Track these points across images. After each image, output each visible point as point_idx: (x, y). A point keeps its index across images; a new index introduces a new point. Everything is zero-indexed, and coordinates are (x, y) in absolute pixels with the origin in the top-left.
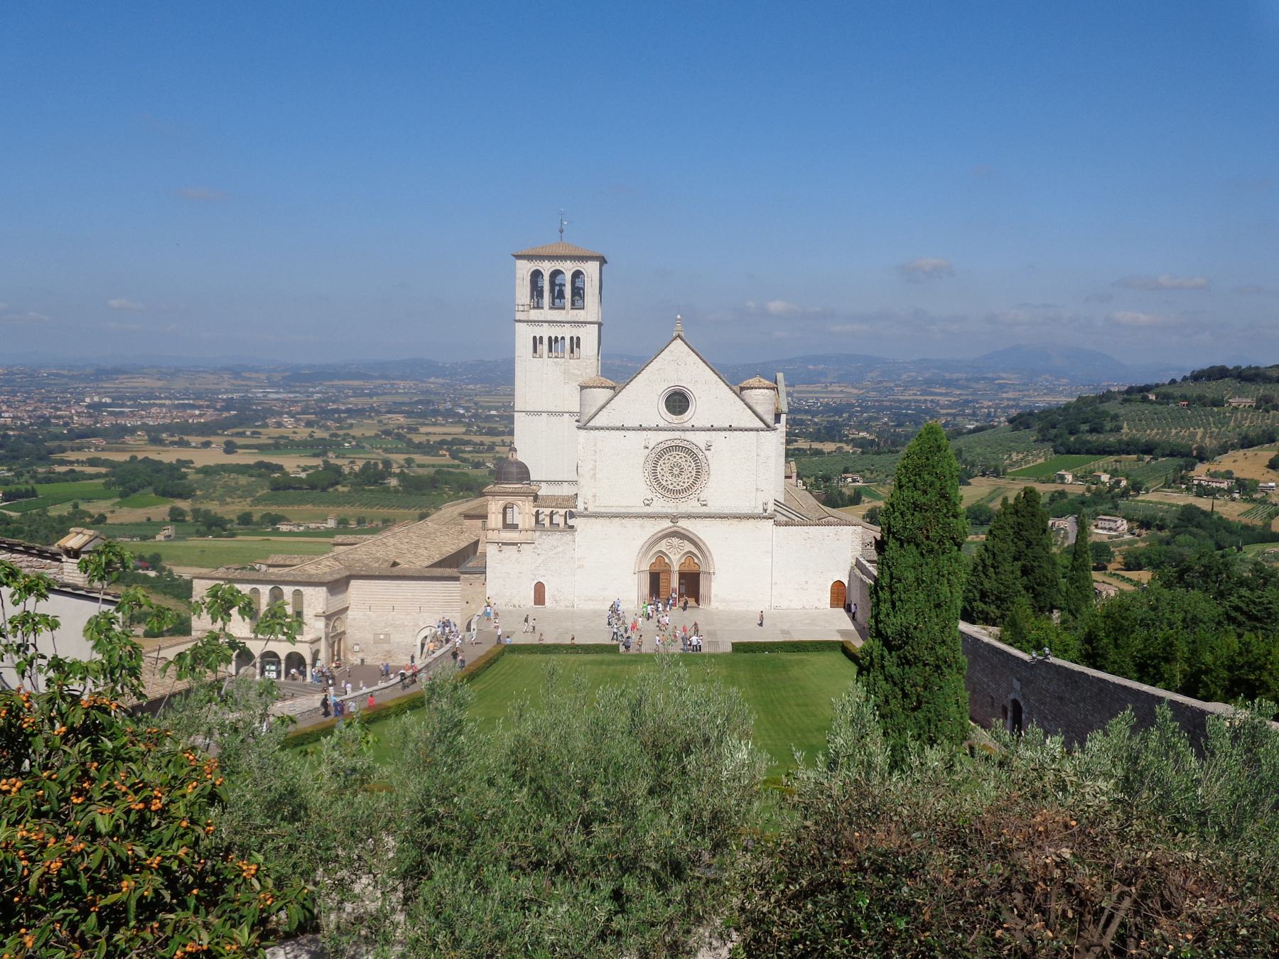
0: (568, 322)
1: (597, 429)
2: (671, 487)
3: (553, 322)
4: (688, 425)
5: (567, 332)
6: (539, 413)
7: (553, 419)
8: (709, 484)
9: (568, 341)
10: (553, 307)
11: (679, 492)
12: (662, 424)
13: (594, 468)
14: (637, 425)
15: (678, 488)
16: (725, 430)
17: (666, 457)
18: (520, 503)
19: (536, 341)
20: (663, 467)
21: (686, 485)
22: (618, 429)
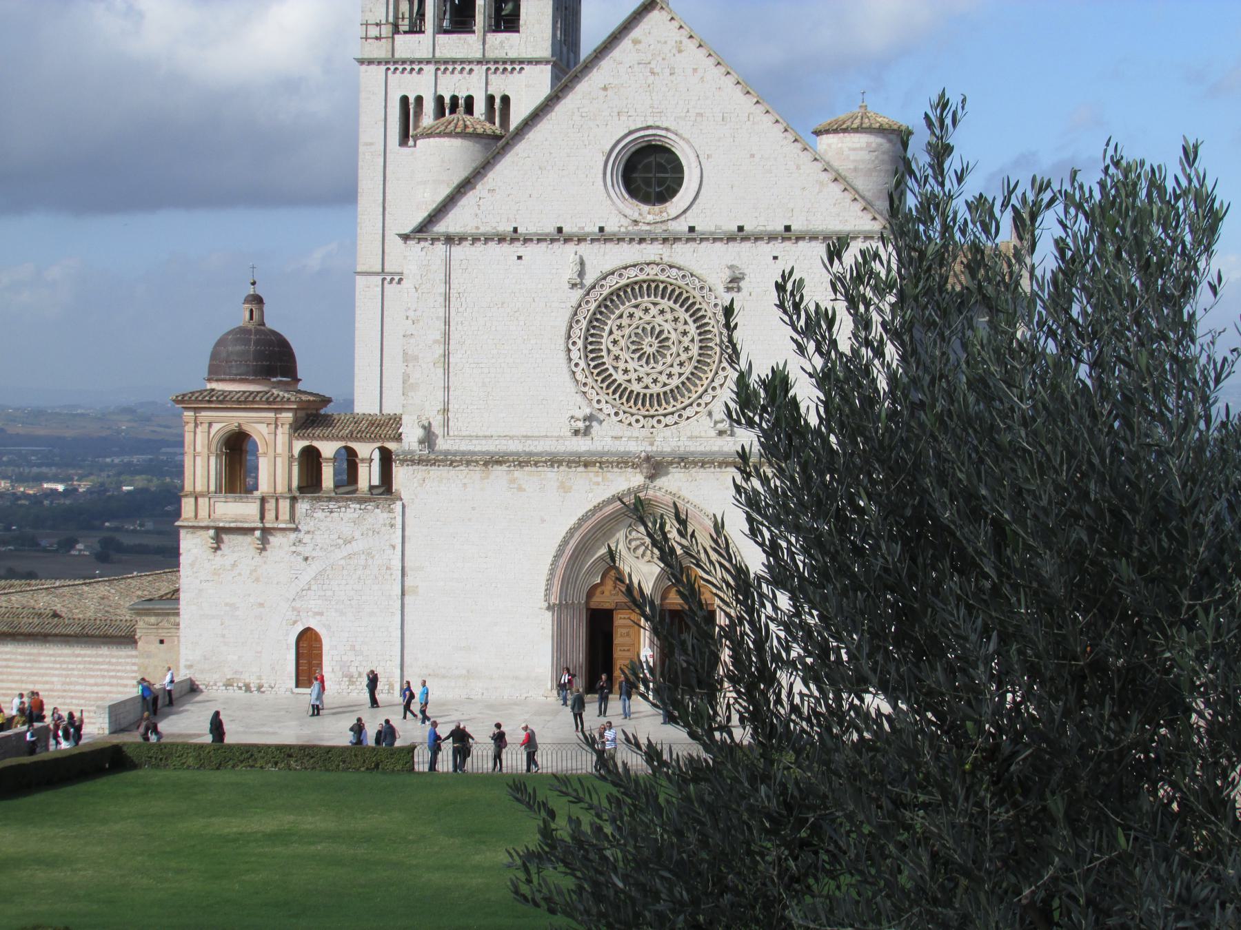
0: (479, 62)
1: (449, 239)
2: (636, 387)
4: (681, 226)
11: (658, 399)
14: (550, 229)
15: (656, 389)
16: (772, 238)
17: (626, 308)
18: (263, 428)
19: (408, 109)
21: (675, 382)
22: (501, 240)
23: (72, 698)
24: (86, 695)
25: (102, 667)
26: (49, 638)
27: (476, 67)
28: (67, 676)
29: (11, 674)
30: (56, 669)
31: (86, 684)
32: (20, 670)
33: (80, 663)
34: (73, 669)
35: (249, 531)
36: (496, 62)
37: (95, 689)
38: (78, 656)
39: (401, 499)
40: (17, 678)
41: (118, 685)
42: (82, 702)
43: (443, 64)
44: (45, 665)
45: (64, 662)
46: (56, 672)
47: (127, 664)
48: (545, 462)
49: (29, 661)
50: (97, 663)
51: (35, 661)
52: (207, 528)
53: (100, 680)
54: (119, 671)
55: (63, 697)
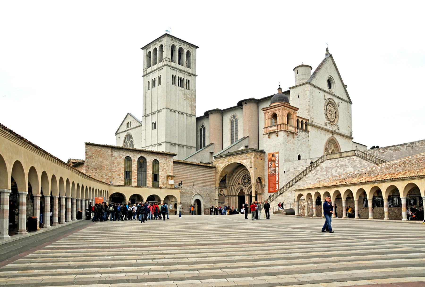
0: (186, 72)
2: (330, 119)
3: (181, 70)
4: (334, 94)
5: (186, 77)
6: (175, 111)
7: (181, 116)
8: (339, 121)
9: (185, 81)
10: (179, 64)
12: (328, 91)
13: (312, 104)
15: (332, 120)
17: (328, 106)
19: (174, 77)
20: (328, 110)
23: (192, 180)
26: (187, 165)
27: (185, 73)
28: (190, 174)
29: (179, 173)
30: (188, 172)
31: (194, 177)
32: (181, 172)
33: (193, 171)
34: (191, 173)
35: (293, 133)
36: (188, 73)
37: (196, 178)
38: (193, 170)
39: (309, 132)
40: (181, 174)
41: (200, 177)
43: (180, 70)
44: (186, 171)
46: (188, 173)
47: (202, 172)
49: (183, 170)
50: (196, 172)
51: (184, 170)
52: (287, 132)
53: (197, 176)
54: (200, 174)
55: (190, 179)
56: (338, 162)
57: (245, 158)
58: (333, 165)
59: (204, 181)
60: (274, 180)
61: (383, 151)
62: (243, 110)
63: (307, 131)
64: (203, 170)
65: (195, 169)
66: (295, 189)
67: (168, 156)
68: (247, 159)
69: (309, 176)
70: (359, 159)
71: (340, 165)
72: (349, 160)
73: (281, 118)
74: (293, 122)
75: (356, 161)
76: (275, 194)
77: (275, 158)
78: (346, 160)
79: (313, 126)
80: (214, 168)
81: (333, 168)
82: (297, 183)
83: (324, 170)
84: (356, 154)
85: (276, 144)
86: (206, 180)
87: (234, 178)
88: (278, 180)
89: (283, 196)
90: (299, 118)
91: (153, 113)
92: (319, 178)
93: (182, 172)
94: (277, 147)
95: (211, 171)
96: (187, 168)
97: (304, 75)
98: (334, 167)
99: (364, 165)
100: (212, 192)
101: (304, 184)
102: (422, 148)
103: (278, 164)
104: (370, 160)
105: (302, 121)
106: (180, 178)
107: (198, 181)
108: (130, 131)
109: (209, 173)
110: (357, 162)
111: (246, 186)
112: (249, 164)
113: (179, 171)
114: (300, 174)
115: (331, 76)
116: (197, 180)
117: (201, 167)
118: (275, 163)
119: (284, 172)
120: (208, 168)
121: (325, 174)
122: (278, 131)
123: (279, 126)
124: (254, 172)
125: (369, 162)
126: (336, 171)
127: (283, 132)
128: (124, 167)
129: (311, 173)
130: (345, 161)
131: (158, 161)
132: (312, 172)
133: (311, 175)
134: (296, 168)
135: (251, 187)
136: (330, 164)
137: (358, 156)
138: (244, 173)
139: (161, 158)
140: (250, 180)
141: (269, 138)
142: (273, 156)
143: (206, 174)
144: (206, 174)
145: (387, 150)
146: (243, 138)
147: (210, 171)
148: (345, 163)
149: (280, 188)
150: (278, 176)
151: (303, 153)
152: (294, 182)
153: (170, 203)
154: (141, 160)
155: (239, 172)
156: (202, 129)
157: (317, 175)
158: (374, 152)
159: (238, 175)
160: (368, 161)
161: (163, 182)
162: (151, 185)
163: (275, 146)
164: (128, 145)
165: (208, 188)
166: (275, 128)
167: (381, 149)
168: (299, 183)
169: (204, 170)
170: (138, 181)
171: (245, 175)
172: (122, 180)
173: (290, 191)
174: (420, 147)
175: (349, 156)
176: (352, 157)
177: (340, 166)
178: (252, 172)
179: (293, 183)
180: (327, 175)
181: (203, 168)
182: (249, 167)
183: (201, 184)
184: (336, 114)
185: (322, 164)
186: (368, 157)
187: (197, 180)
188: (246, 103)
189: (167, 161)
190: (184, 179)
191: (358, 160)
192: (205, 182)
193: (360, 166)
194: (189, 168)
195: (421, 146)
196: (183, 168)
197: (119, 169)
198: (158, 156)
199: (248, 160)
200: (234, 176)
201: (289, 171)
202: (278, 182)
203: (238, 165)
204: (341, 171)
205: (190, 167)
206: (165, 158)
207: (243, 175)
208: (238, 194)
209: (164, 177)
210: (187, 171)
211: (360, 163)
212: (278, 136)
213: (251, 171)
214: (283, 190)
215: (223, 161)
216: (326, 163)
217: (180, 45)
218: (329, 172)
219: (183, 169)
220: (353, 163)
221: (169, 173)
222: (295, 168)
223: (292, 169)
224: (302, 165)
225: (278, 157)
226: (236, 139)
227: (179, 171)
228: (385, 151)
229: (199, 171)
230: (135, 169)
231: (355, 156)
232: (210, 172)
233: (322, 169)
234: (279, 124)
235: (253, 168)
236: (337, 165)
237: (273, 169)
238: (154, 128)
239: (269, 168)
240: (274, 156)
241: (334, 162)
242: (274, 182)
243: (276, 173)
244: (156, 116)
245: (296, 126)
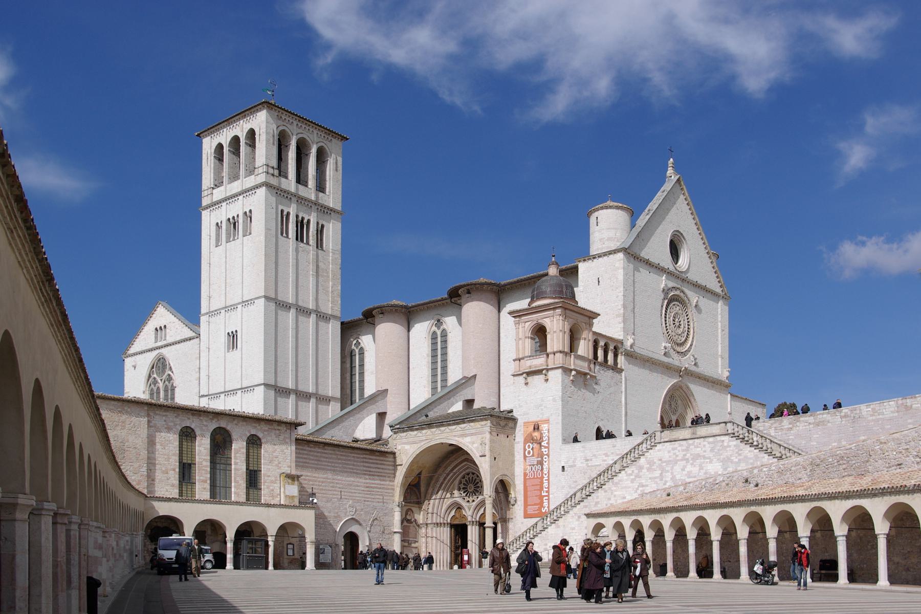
15: (679, 342)
21: (683, 339)
23: (337, 483)
24: (343, 482)
25: (350, 467)
26: (326, 447)
33: (340, 463)
34: (337, 467)
38: (339, 459)
42: (341, 486)
45: (333, 463)
46: (329, 468)
48: (659, 364)
49: (316, 460)
50: (347, 464)
54: (357, 470)
56: (687, 450)
57: (467, 432)
58: (677, 456)
59: (367, 487)
60: (538, 487)
61: (791, 426)
62: (461, 309)
63: (615, 368)
64: (364, 460)
65: (344, 458)
66: (587, 511)
67: (284, 425)
68: (472, 434)
69: (620, 481)
70: (735, 442)
71: (691, 455)
72: (712, 445)
73: (555, 337)
74: (584, 348)
75: (730, 446)
76: (540, 522)
77: (541, 434)
78: (706, 444)
79: (631, 356)
80: (392, 456)
81: (676, 462)
82: (592, 495)
83: (654, 467)
84: (729, 432)
85: (542, 401)
86: (373, 484)
87: (441, 479)
88: (548, 488)
89: (558, 527)
90: (599, 338)
91: (232, 308)
92: (643, 486)
93: (313, 464)
94: (545, 407)
95: (385, 463)
96: (327, 456)
97: (613, 229)
98: (678, 460)
99: (746, 457)
100: (386, 514)
101: (609, 499)
102: (873, 420)
103: (547, 450)
104: (760, 446)
105: (606, 345)
106: (310, 480)
107: (353, 488)
108: (164, 351)
109: (379, 468)
110: (731, 449)
111: (471, 499)
112: (477, 448)
113: (306, 463)
114: (600, 475)
115: (678, 231)
116: (351, 485)
117: (359, 452)
118: (541, 446)
119: (563, 467)
120: (378, 456)
121: (659, 475)
122: (548, 370)
123: (551, 356)
124: (491, 467)
125: (757, 450)
126: (683, 470)
127: (560, 371)
128: (178, 452)
129: (626, 472)
130: (704, 446)
131: (260, 439)
132: (628, 470)
133: (625, 478)
134: (591, 460)
135: (482, 503)
136: (669, 452)
137: (732, 437)
138: (465, 470)
139: (267, 431)
140: (479, 487)
141: (526, 384)
142: (537, 428)
143: (371, 470)
144: (371, 470)
145: (798, 424)
146: (461, 379)
147: (383, 462)
148: (705, 451)
149: (552, 507)
150: (548, 477)
151: (609, 421)
152: (587, 491)
153: (289, 542)
154: (217, 437)
155: (452, 466)
156: (357, 351)
157: (640, 477)
158: (770, 428)
159: (448, 475)
160: (755, 449)
161: (273, 490)
162: (243, 498)
163: (541, 405)
164: (158, 388)
165: (377, 504)
166: (539, 362)
167: (785, 422)
168: (598, 497)
169: (367, 460)
170: (211, 486)
171: (468, 474)
172: (173, 485)
173: (575, 514)
174: (871, 418)
175: (714, 436)
176: (719, 438)
177: (692, 459)
178: (485, 468)
179: (584, 496)
180: (661, 480)
181: (364, 456)
182: (478, 455)
183: (361, 495)
184: (688, 325)
185: (650, 451)
186: (755, 439)
187: (351, 485)
188: (469, 292)
189: (282, 438)
190: (319, 482)
191: (732, 446)
192: (370, 489)
193: (737, 460)
194: (331, 454)
195: (872, 415)
196: (315, 454)
197: (166, 457)
198: (259, 427)
199: (474, 437)
200: (441, 475)
201: (575, 466)
202: (547, 492)
203: (451, 448)
204: (695, 470)
205: (333, 452)
206: (278, 432)
207: (462, 474)
208: (449, 521)
209: (273, 479)
210: (326, 462)
211: (737, 453)
212: (547, 380)
213: (483, 465)
214: (558, 511)
215: (416, 439)
216: (659, 450)
217: (300, 131)
218: (668, 471)
219: (317, 456)
220: (721, 452)
221: (286, 468)
222: (587, 460)
223: (582, 463)
224: (605, 452)
225: (548, 432)
226: (444, 380)
227: (308, 463)
228: (793, 426)
229: (355, 461)
230: (206, 458)
231: (725, 435)
232: (381, 464)
233: (651, 463)
234: (552, 351)
235: (487, 458)
236: (685, 455)
237: (534, 460)
238: (233, 348)
239: (525, 457)
240: (538, 428)
241: (679, 448)
242: (538, 493)
243: (542, 469)
244: (240, 316)
245: (591, 357)
